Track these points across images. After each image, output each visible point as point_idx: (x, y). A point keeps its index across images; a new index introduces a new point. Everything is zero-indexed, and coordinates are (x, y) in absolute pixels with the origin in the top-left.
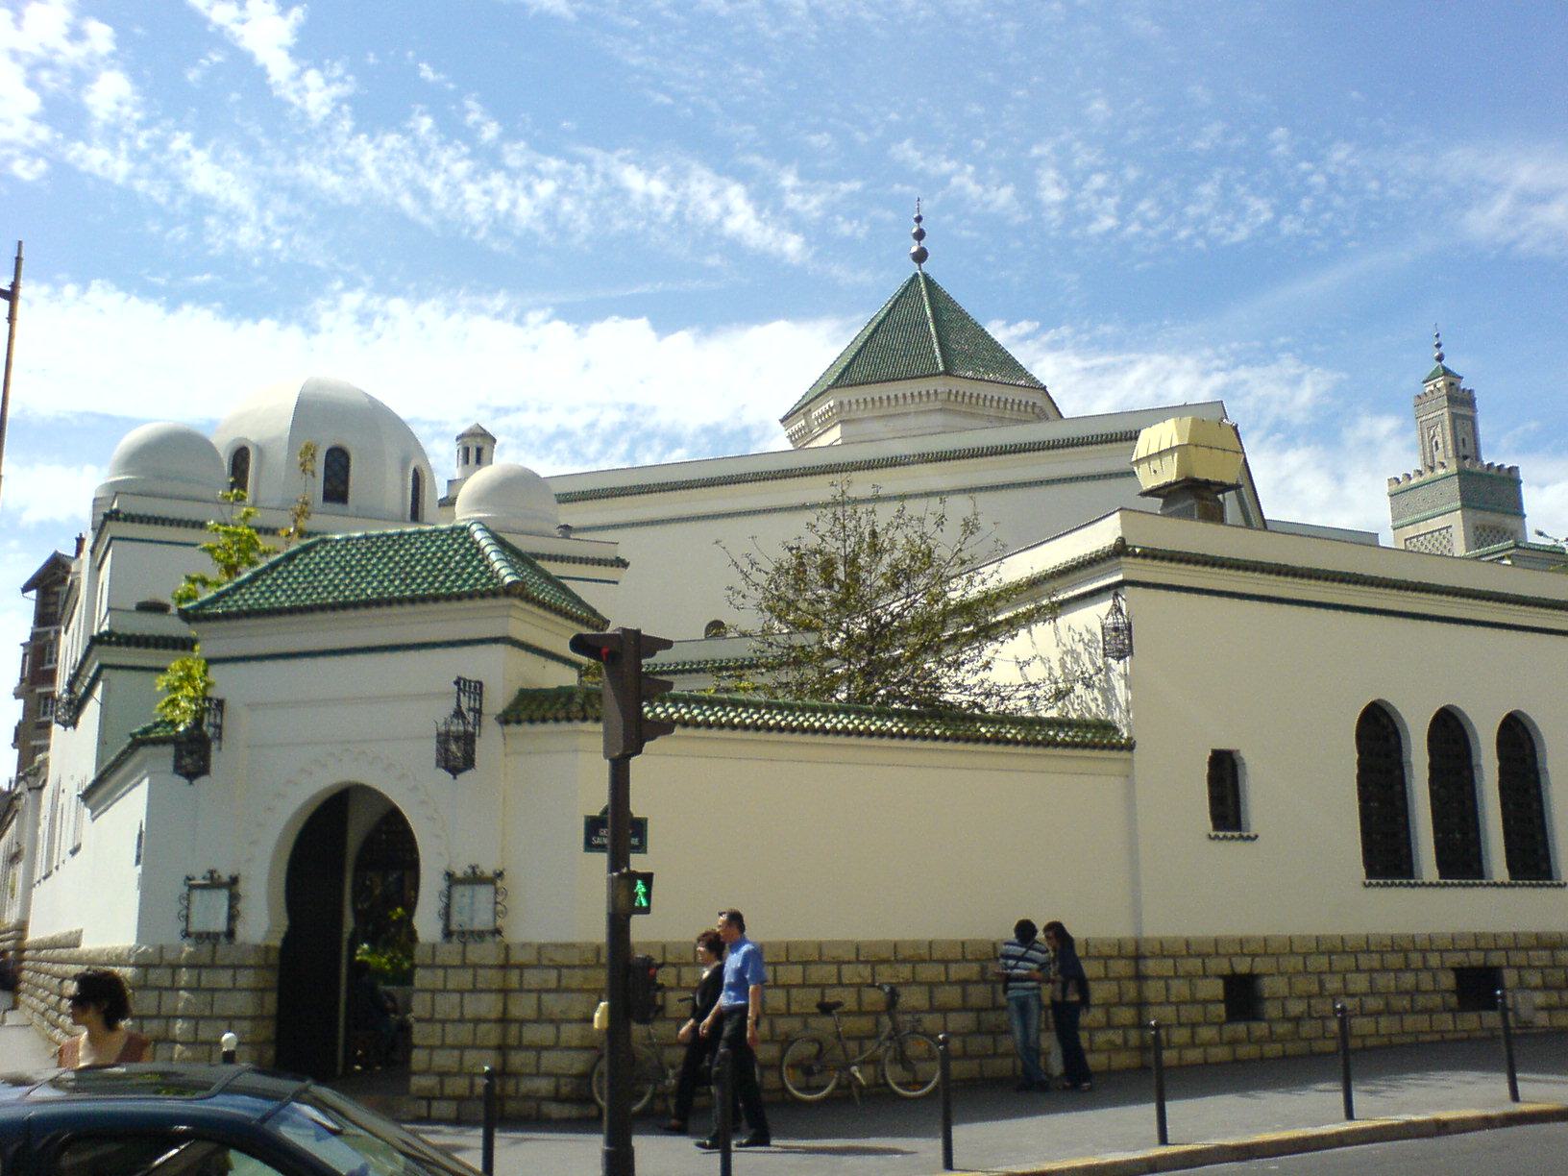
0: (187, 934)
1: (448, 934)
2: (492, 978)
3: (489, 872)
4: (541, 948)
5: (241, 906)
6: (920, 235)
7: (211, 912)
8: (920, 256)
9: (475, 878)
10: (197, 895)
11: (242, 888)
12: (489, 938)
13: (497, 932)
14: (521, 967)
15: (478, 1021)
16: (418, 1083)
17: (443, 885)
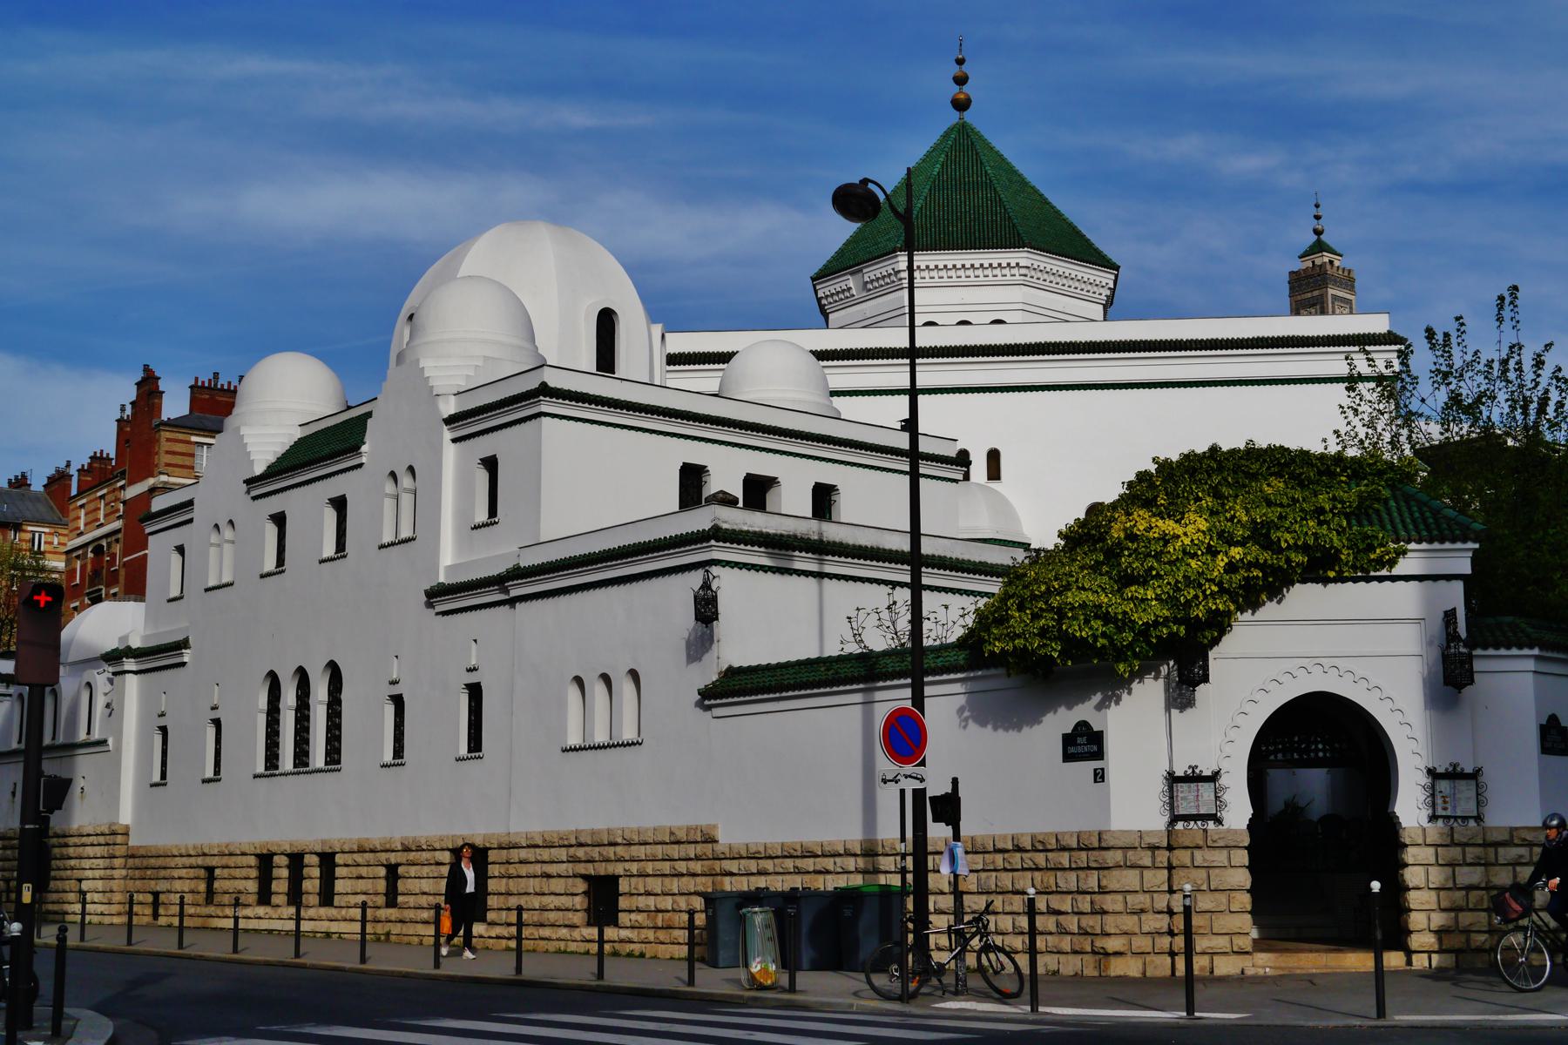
0: (1175, 819)
1: (1433, 818)
2: (1472, 853)
3: (1468, 770)
4: (1512, 830)
5: (1226, 797)
6: (961, 80)
7: (1194, 799)
8: (961, 105)
9: (1454, 775)
10: (1182, 788)
11: (1223, 780)
12: (1472, 823)
13: (1478, 818)
14: (1497, 845)
15: (1469, 888)
16: (1415, 941)
17: (1424, 780)
